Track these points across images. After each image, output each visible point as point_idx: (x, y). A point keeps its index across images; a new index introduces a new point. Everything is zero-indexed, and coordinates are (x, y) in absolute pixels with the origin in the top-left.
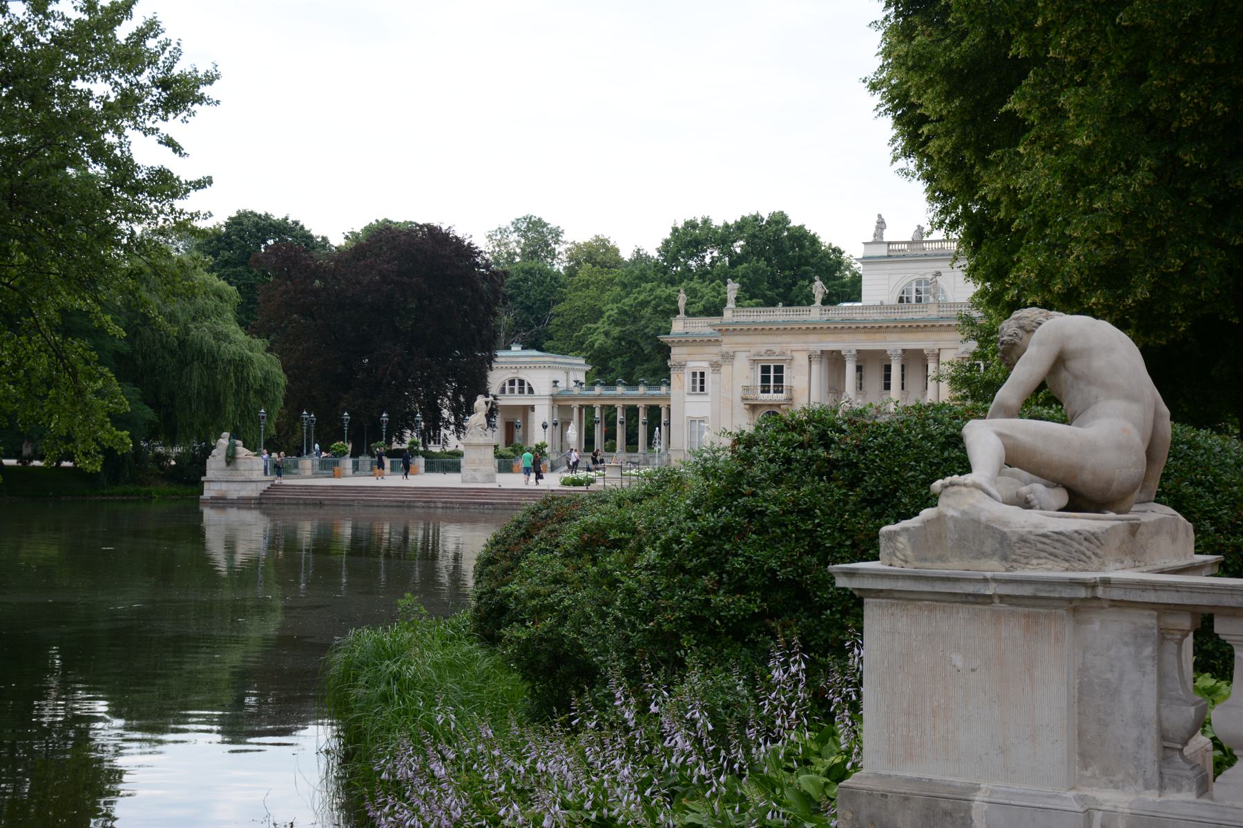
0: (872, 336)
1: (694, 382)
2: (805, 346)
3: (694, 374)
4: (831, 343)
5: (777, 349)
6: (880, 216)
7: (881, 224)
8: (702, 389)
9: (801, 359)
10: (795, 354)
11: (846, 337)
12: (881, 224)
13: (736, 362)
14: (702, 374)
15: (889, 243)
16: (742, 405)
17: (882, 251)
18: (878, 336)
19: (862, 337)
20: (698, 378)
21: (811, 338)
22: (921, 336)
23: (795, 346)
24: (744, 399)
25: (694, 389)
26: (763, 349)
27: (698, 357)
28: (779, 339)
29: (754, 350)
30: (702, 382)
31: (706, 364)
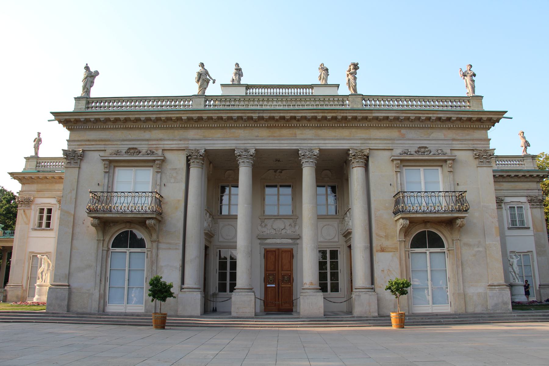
0: (277, 132)
1: (41, 218)
2: (182, 144)
3: (42, 210)
4: (219, 141)
5: (143, 147)
6: (237, 64)
7: (239, 72)
8: (48, 225)
9: (177, 161)
10: (168, 155)
11: (241, 132)
12: (239, 72)
13: (84, 165)
14: (50, 211)
15: (248, 87)
16: (89, 220)
17: (241, 92)
18: (285, 132)
19: (264, 133)
20: (45, 214)
21: (192, 133)
22: (345, 132)
23: (168, 144)
24: (90, 211)
25: (40, 225)
26: (124, 148)
27: (47, 194)
28: (147, 135)
29: (111, 149)
30: (49, 218)
31: (53, 201)
